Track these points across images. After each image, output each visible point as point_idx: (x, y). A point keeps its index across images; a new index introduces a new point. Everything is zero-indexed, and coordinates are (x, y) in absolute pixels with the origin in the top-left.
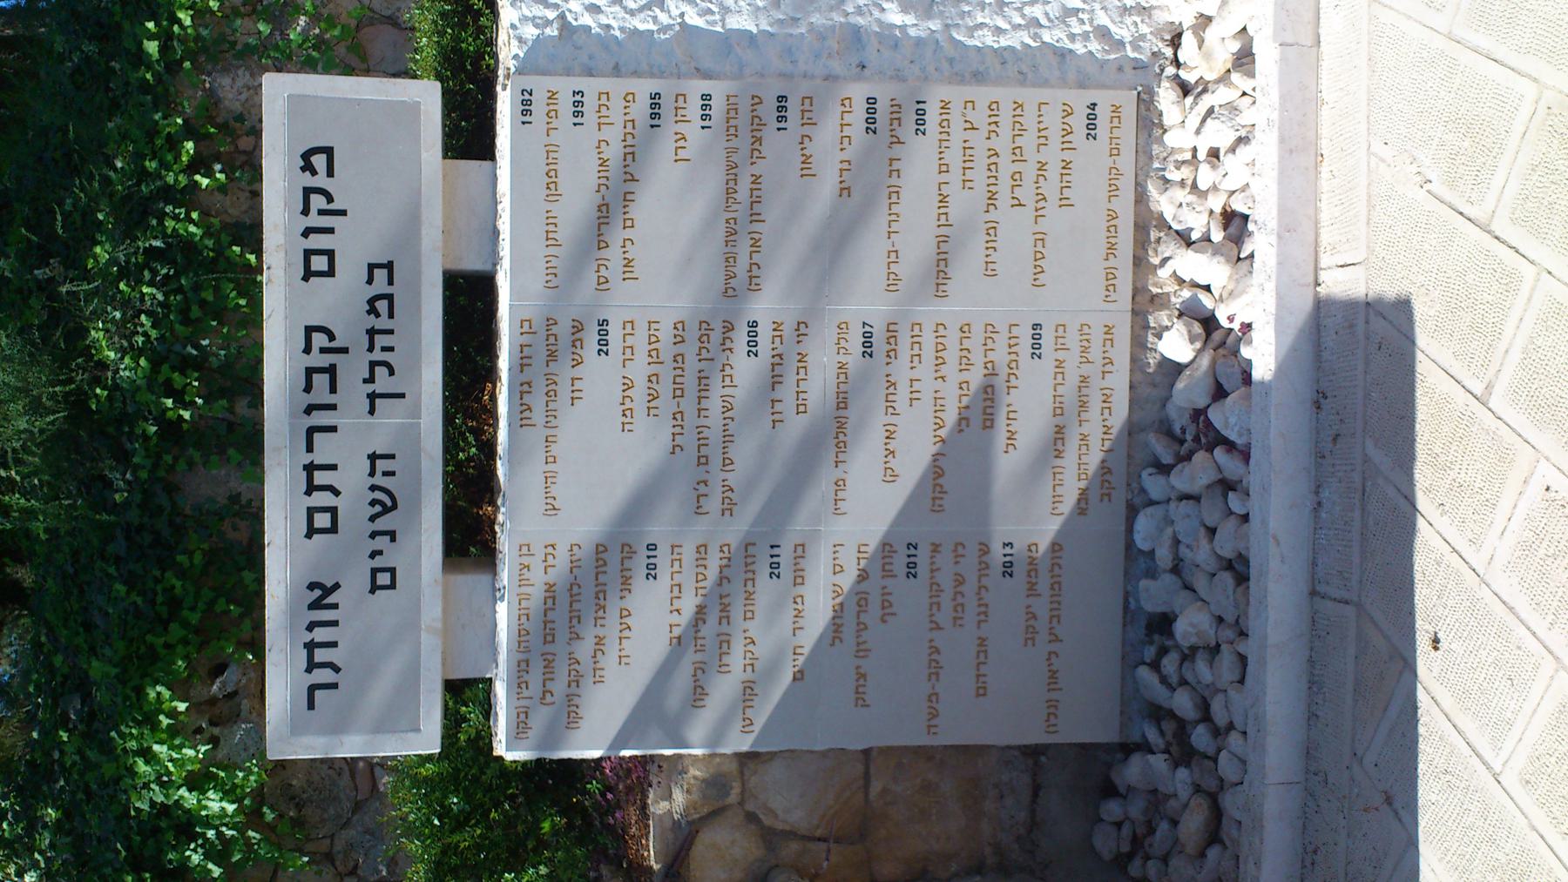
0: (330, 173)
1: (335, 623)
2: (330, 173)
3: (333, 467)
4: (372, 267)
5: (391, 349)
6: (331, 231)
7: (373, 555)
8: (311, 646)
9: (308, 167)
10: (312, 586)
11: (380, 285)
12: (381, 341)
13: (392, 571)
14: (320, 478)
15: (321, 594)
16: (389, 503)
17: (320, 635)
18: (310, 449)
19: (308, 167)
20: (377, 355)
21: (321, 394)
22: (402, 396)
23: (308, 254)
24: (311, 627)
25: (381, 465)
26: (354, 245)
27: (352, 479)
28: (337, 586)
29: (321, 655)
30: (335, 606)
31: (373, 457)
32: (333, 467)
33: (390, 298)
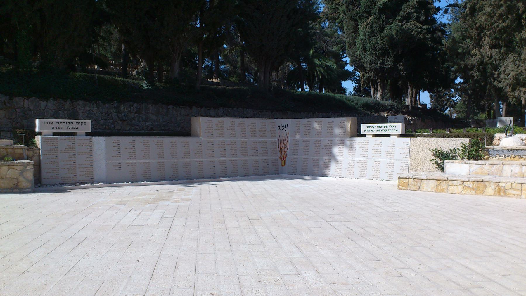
15: (52, 123)
26: (79, 126)
27: (61, 125)
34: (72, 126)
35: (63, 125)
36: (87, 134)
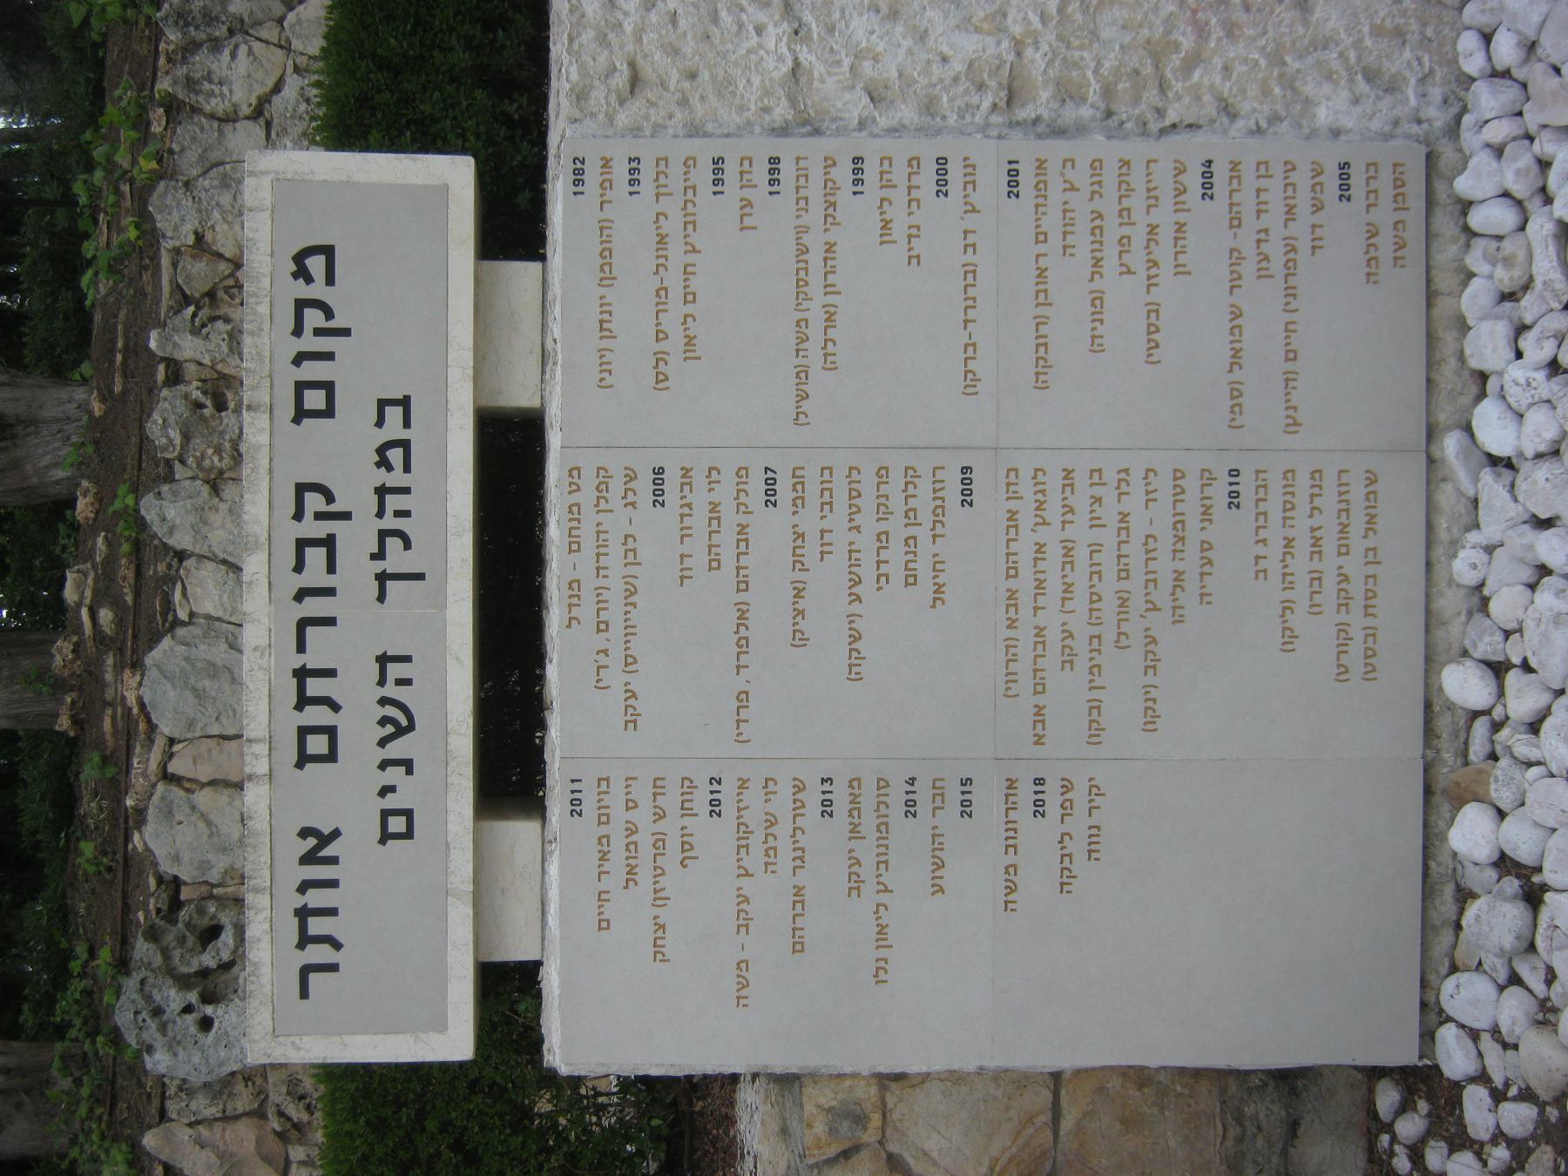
0: (330, 280)
1: (333, 884)
2: (330, 280)
3: (331, 673)
4: (382, 404)
5: (406, 514)
6: (329, 356)
7: (386, 791)
8: (303, 914)
9: (302, 273)
10: (305, 833)
11: (393, 428)
12: (393, 502)
13: (408, 814)
14: (315, 687)
15: (319, 845)
16: (404, 723)
17: (316, 898)
18: (301, 647)
19: (302, 273)
20: (389, 522)
21: (316, 573)
22: (420, 577)
23: (301, 387)
24: (304, 887)
25: (394, 670)
26: (358, 375)
27: (357, 693)
28: (336, 834)
29: (316, 926)
30: (333, 861)
31: (383, 660)
32: (331, 673)
33: (405, 445)
34: (355, 493)
35: (345, 651)
36: (512, 224)
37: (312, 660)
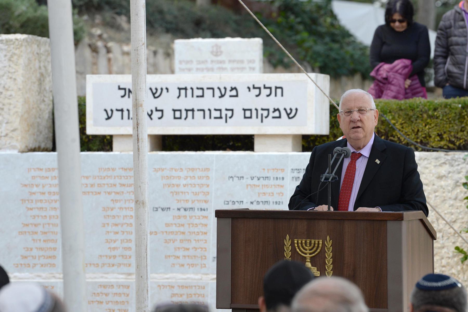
2: (273, 117)
6: (257, 117)
37: (196, 113)
